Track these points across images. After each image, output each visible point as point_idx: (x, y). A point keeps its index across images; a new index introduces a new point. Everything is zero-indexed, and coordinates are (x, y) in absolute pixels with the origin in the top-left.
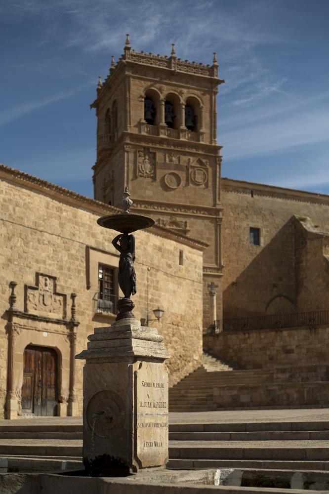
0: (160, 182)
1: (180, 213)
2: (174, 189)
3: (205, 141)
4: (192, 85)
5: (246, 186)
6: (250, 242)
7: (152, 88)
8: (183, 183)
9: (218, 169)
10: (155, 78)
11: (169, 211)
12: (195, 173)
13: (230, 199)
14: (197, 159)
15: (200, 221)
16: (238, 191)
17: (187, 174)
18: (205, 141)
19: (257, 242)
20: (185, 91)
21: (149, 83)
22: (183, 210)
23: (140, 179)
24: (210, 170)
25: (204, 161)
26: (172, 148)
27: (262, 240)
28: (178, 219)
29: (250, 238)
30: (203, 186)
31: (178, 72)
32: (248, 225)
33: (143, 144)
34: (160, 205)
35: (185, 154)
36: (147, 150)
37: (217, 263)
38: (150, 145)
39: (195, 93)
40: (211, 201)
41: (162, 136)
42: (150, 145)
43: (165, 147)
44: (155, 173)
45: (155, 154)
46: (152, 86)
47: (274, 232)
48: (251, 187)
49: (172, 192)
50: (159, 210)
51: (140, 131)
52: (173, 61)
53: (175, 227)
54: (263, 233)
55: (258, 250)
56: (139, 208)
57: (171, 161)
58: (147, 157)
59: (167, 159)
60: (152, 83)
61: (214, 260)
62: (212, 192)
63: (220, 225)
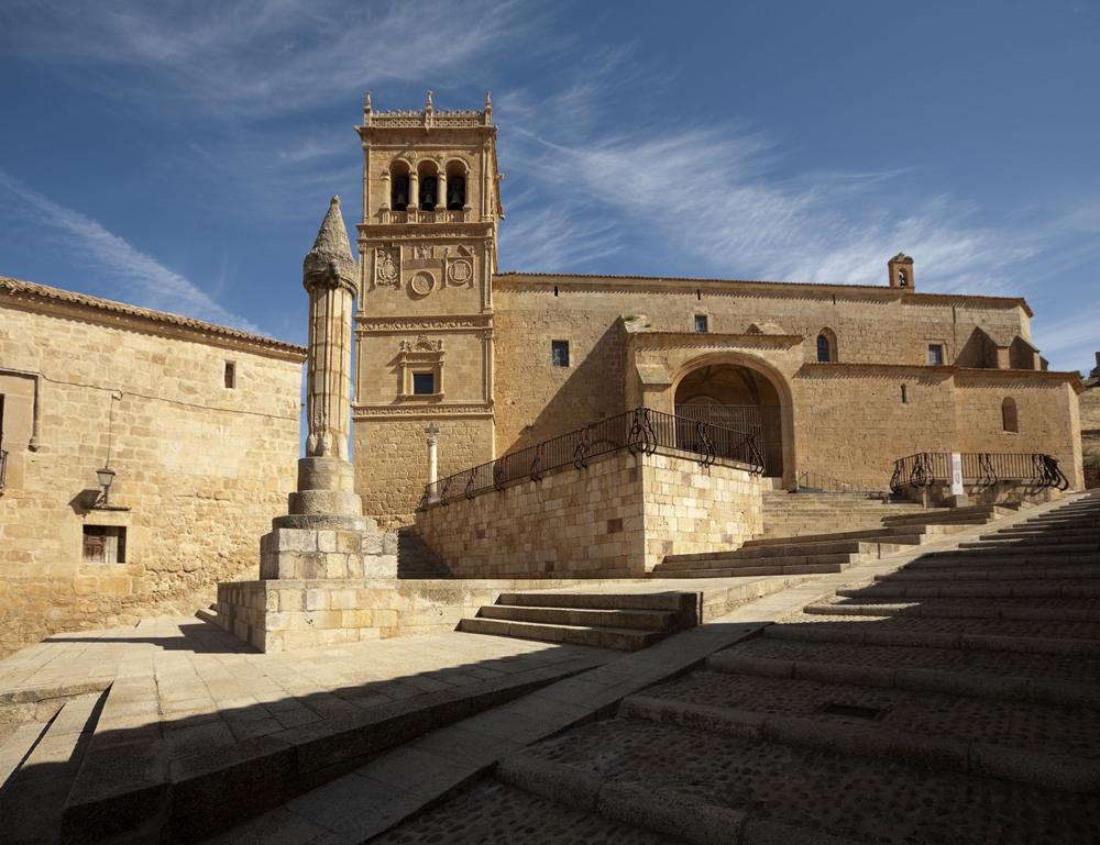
0: (407, 288)
1: (432, 328)
2: (424, 296)
3: (471, 218)
4: (454, 143)
5: (546, 280)
6: (554, 364)
7: (400, 159)
8: (436, 284)
9: (487, 257)
10: (404, 143)
11: (418, 327)
12: (453, 267)
13: (522, 303)
14: (457, 247)
15: (461, 337)
16: (535, 290)
17: (444, 272)
18: (471, 218)
19: (564, 363)
20: (443, 154)
21: (395, 153)
22: (437, 324)
23: (378, 288)
24: (476, 259)
25: (467, 248)
26: (423, 236)
27: (571, 358)
28: (430, 338)
29: (554, 357)
30: (467, 284)
31: (431, 129)
32: (549, 337)
33: (384, 238)
34: (404, 320)
35: (440, 242)
36: (388, 245)
37: (484, 398)
38: (394, 238)
39: (460, 154)
40: (478, 307)
41: (409, 222)
42: (394, 238)
43: (414, 236)
44: (399, 275)
45: (399, 249)
46: (399, 156)
47: (590, 345)
48: (554, 280)
49: (422, 301)
50: (404, 328)
51: (381, 221)
52: (427, 115)
53: (424, 350)
54: (573, 347)
55: (565, 374)
56: (376, 329)
57: (421, 255)
58: (389, 256)
59: (416, 256)
60: (399, 152)
61: (481, 392)
62: (478, 291)
63: (489, 340)
